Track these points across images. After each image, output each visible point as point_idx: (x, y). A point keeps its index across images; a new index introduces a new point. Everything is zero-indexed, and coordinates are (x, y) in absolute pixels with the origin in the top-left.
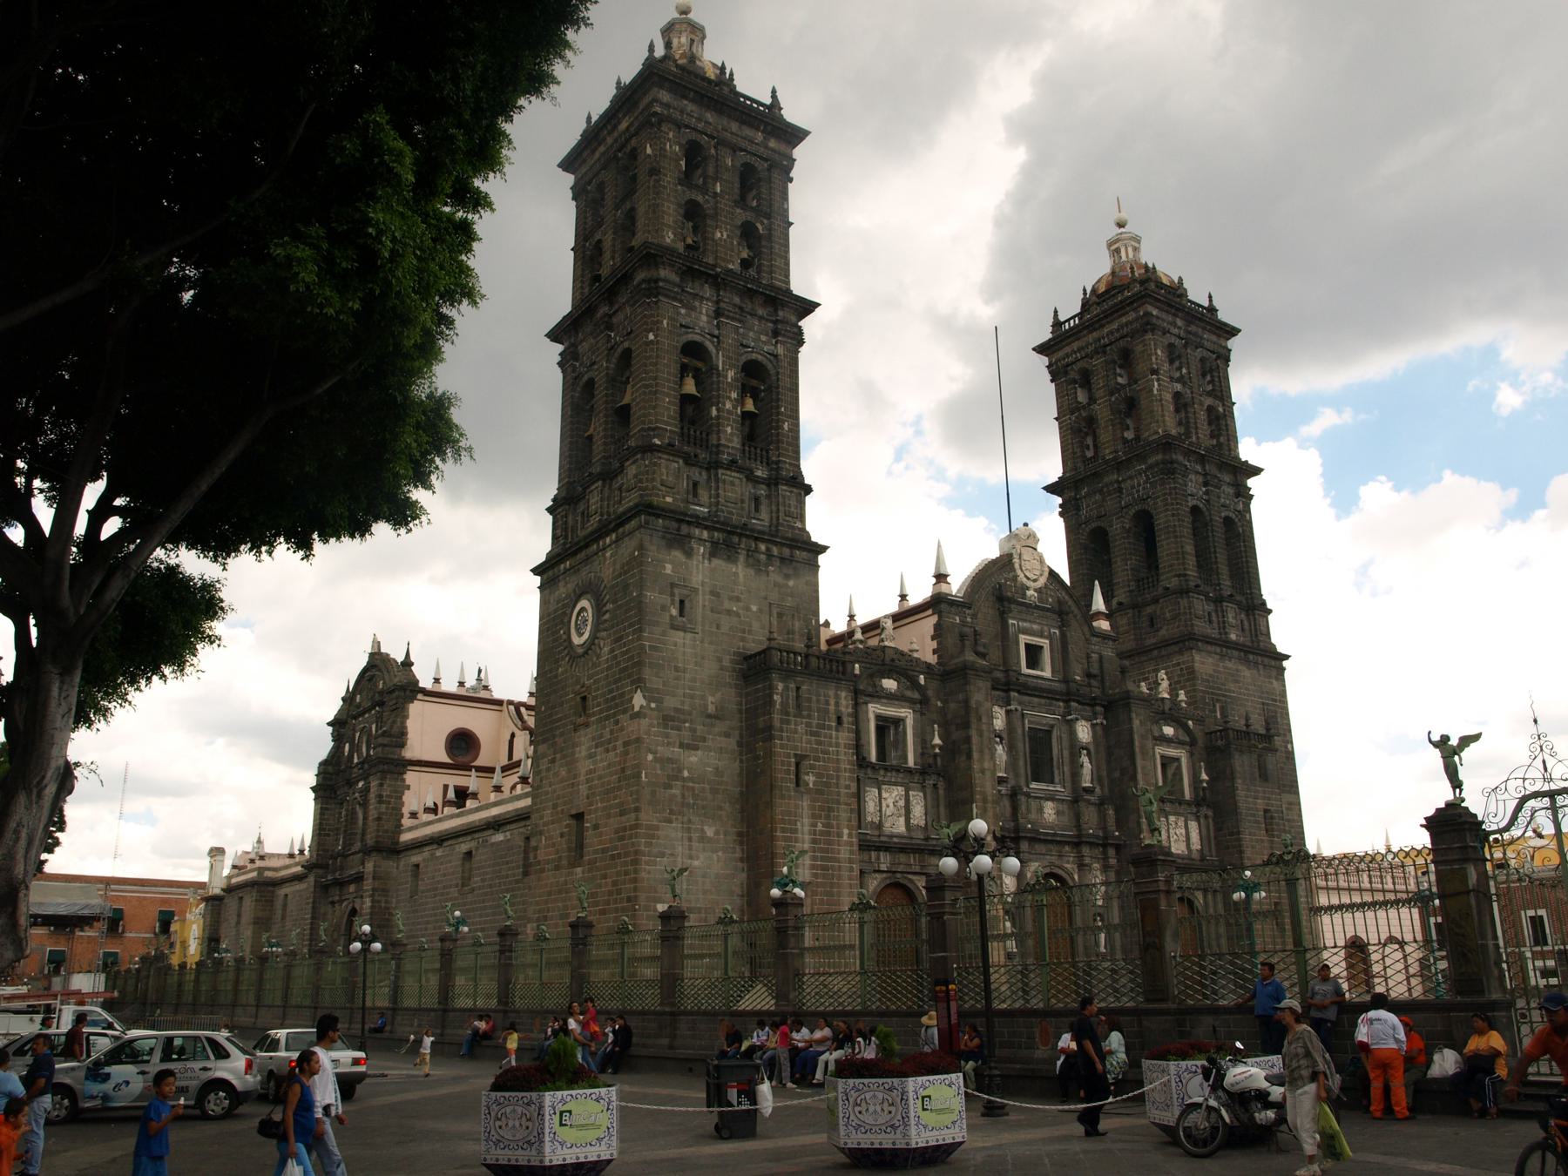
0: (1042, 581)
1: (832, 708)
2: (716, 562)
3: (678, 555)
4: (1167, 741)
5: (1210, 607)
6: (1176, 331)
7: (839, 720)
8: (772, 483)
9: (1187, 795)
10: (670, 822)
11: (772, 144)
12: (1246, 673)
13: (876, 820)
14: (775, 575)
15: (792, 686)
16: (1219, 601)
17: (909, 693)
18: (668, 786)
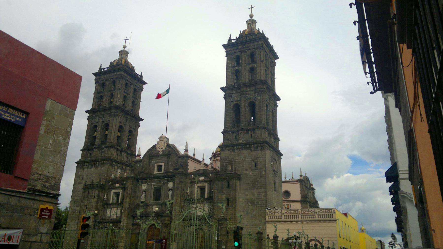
0: (164, 148)
1: (93, 195)
2: (89, 169)
3: (82, 170)
4: (200, 182)
5: (235, 134)
6: (238, 51)
7: (94, 197)
8: (103, 148)
9: (206, 197)
10: (72, 221)
11: (118, 73)
12: (245, 152)
13: (109, 216)
14: (99, 168)
15: (87, 192)
16: (238, 131)
17: (121, 186)
18: (73, 214)
